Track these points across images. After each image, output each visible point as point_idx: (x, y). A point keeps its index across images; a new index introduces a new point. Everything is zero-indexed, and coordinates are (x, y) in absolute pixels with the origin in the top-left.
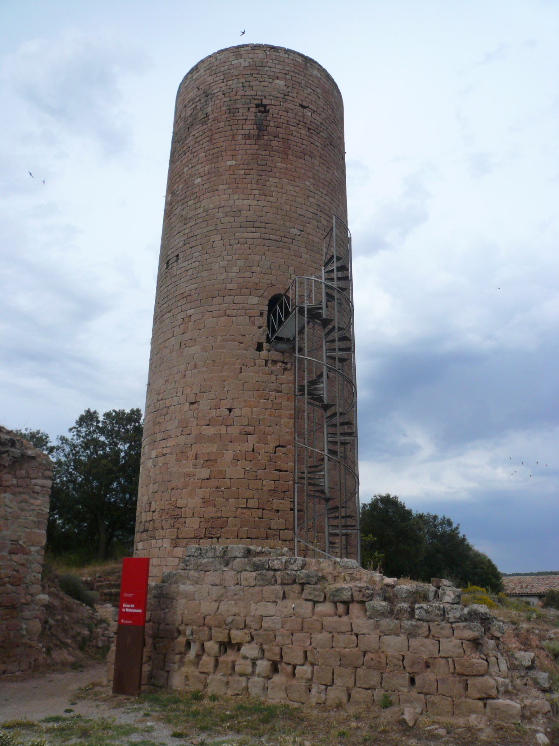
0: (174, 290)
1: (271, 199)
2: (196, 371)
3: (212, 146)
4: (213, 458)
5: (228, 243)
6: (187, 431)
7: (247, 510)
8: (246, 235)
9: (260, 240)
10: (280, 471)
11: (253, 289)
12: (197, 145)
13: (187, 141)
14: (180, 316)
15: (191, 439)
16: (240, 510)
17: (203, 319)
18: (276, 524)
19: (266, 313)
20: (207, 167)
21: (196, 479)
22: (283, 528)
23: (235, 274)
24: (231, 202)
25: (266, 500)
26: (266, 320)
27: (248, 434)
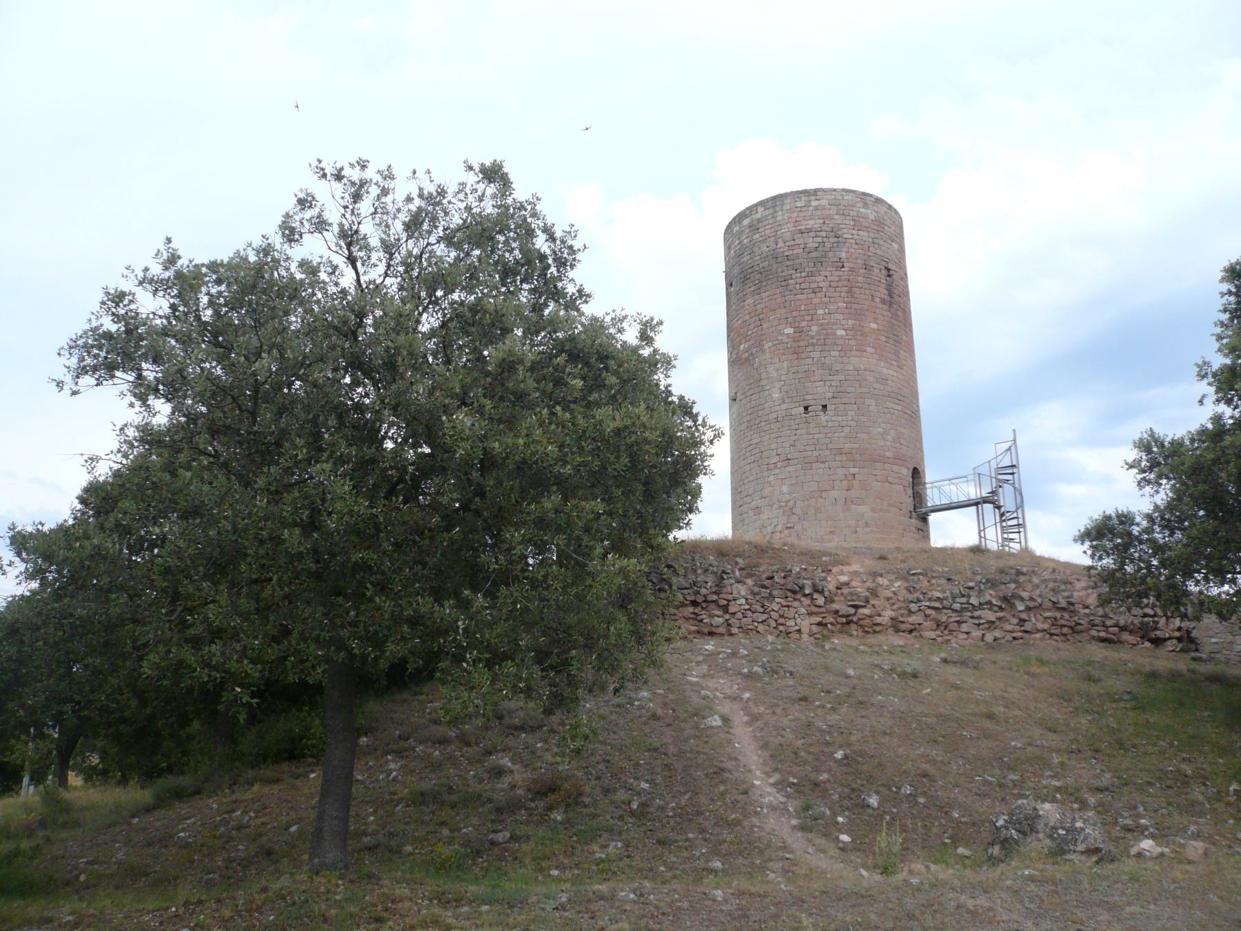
14: (841, 472)
20: (851, 322)
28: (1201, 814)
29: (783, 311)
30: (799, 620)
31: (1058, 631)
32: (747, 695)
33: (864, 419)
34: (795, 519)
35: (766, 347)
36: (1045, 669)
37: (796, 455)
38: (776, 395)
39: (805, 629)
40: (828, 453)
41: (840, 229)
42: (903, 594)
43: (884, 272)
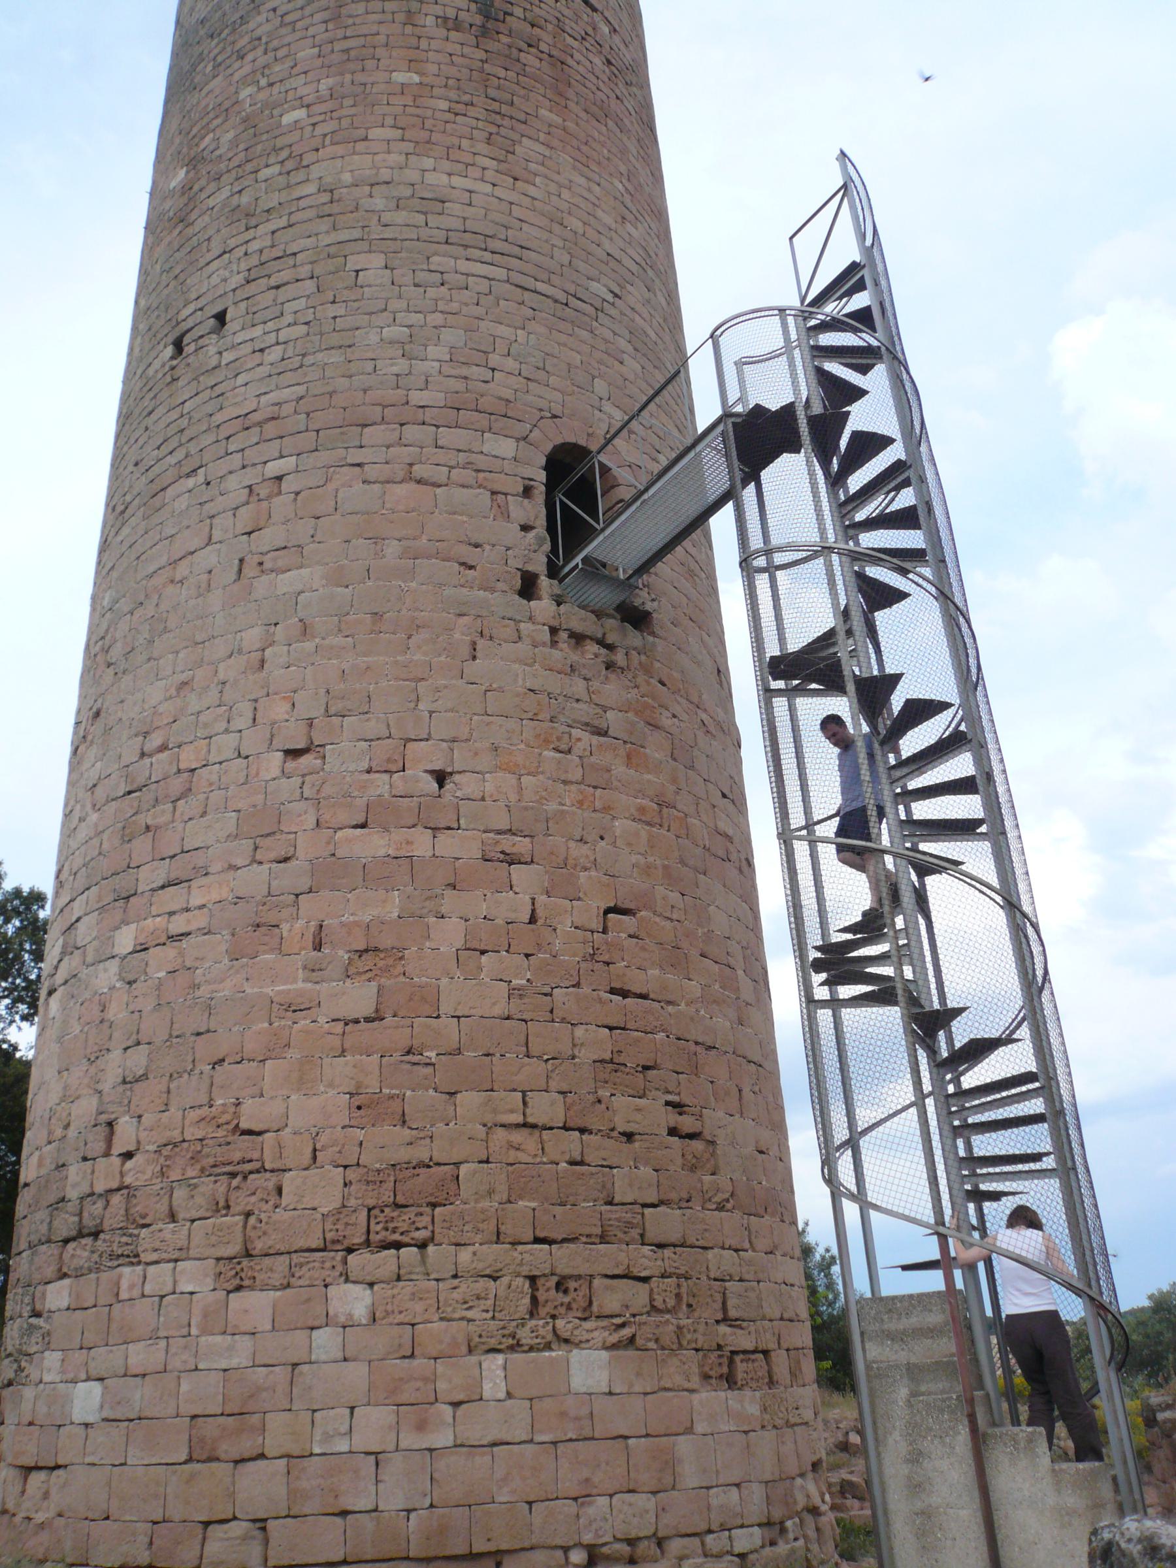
0: (209, 408)
1: (532, 191)
2: (309, 646)
3: (340, 33)
4: (386, 942)
5: (408, 279)
6: (275, 847)
7: (526, 1131)
8: (463, 266)
9: (508, 286)
10: (625, 994)
11: (500, 416)
12: (283, 31)
13: (252, 25)
15: (294, 876)
16: (500, 1133)
17: (331, 487)
18: (631, 1185)
19: (540, 491)
21: (322, 1020)
22: (654, 1200)
23: (436, 364)
24: (412, 175)
25: (591, 1098)
26: (544, 511)
27: (511, 860)
33: (332, 310)
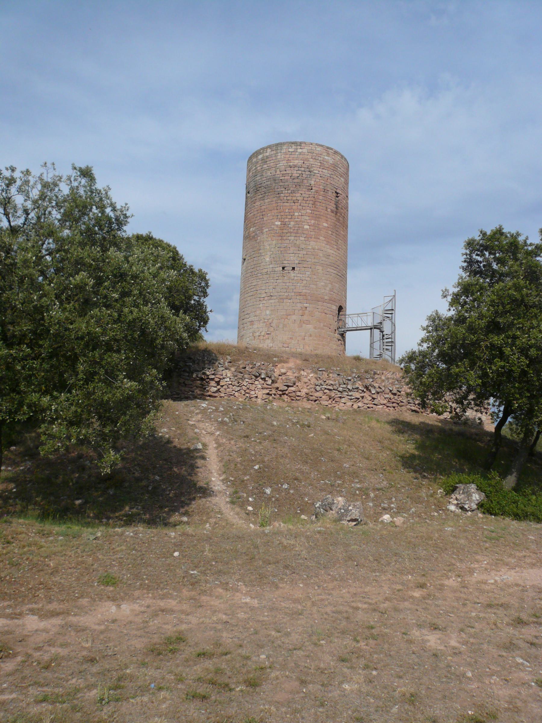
1: (340, 252)
28: (421, 503)
29: (276, 211)
30: (257, 392)
31: (391, 405)
32: (218, 433)
33: (315, 277)
34: (272, 329)
35: (265, 231)
36: (379, 425)
37: (276, 294)
38: (268, 259)
39: (260, 396)
40: (293, 294)
41: (312, 167)
42: (313, 381)
43: (335, 194)
